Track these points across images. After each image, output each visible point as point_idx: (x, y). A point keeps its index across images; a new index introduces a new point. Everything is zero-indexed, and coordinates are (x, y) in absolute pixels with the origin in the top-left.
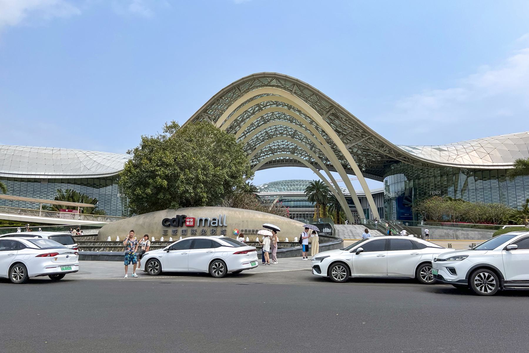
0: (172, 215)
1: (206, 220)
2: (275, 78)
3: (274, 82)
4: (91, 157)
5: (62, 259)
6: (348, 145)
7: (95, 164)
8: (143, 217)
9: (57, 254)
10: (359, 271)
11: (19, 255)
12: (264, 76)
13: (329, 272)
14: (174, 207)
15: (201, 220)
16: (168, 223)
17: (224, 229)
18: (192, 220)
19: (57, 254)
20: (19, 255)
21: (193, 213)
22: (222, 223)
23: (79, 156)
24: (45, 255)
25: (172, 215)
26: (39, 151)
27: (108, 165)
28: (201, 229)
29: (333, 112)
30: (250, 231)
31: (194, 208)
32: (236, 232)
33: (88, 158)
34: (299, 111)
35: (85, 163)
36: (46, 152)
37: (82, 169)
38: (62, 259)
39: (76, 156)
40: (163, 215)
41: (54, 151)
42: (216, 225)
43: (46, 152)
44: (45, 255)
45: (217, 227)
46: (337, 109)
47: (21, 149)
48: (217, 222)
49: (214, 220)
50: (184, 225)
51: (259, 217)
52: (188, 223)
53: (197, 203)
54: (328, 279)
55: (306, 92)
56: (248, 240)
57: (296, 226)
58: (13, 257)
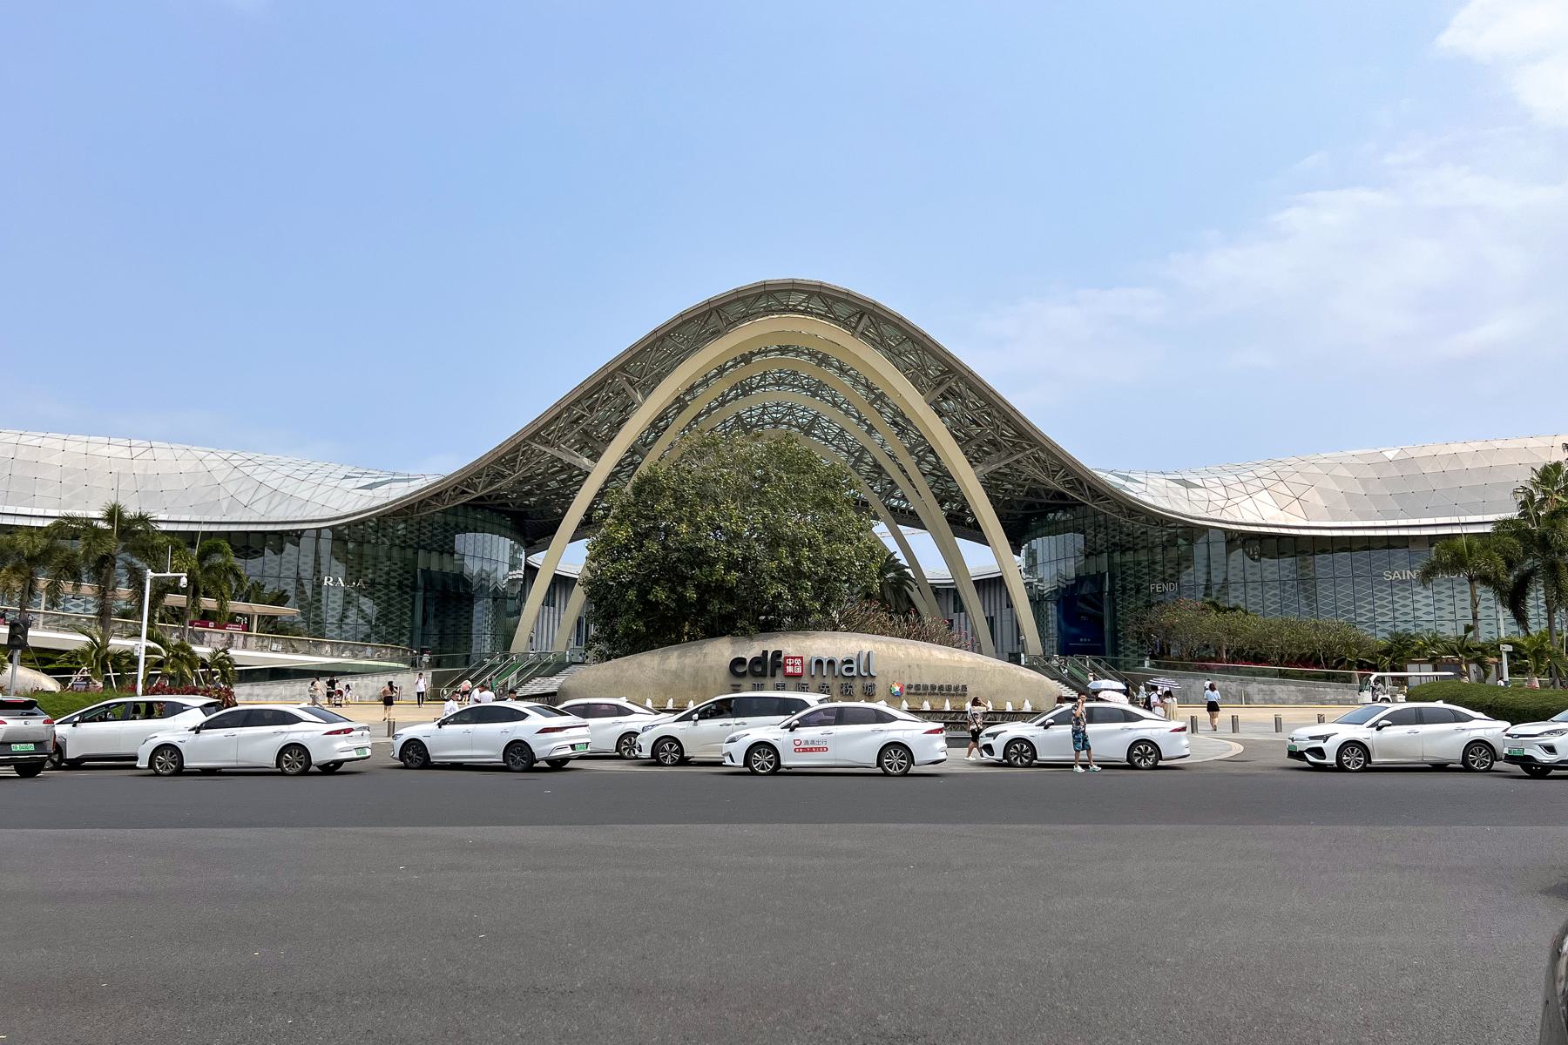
0: (752, 650)
1: (831, 663)
2: (819, 294)
3: (816, 304)
4: (248, 470)
5: (357, 737)
6: (980, 468)
7: (264, 491)
8: (676, 654)
9: (351, 730)
10: (1382, 755)
11: (292, 733)
12: (793, 287)
13: (1339, 758)
14: (745, 633)
15: (819, 662)
16: (740, 670)
17: (869, 682)
18: (798, 662)
19: (351, 730)
20: (292, 733)
21: (795, 646)
22: (868, 669)
23: (211, 466)
24: (338, 732)
25: (752, 650)
26: (91, 449)
27: (306, 495)
28: (819, 681)
29: (948, 381)
30: (925, 687)
31: (791, 636)
32: (897, 689)
33: (237, 474)
34: (842, 370)
35: (231, 488)
36: (113, 451)
37: (225, 504)
38: (357, 737)
39: (201, 468)
40: (721, 652)
41: (136, 451)
42: (855, 673)
43: (113, 451)
44: (338, 732)
45: (850, 679)
46: (962, 378)
47: (36, 442)
48: (854, 666)
49: (850, 662)
50: (779, 672)
51: (942, 656)
52: (790, 669)
53: (802, 622)
54: (1340, 768)
55: (887, 330)
56: (927, 706)
57: (1022, 678)
58: (1465, 734)
